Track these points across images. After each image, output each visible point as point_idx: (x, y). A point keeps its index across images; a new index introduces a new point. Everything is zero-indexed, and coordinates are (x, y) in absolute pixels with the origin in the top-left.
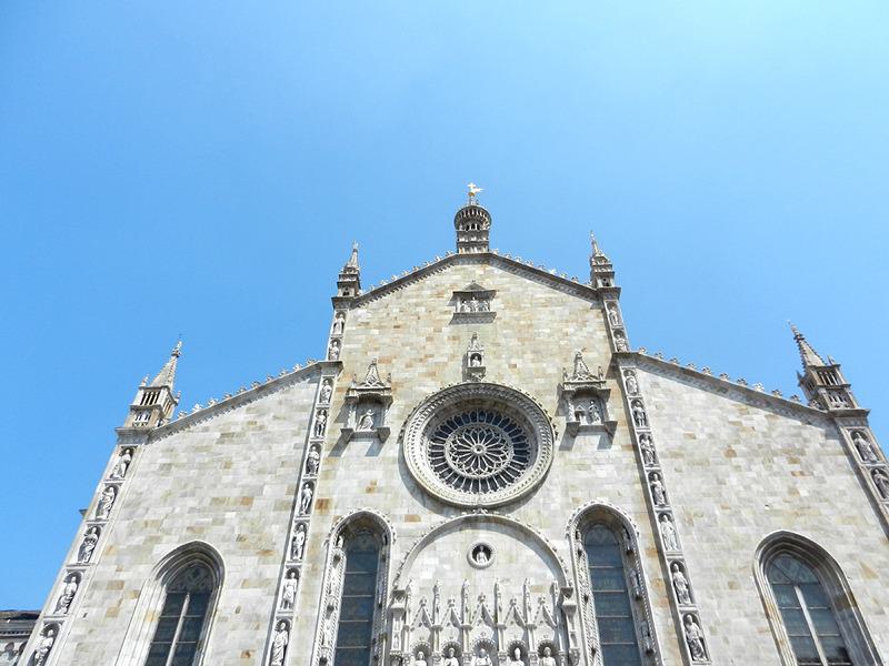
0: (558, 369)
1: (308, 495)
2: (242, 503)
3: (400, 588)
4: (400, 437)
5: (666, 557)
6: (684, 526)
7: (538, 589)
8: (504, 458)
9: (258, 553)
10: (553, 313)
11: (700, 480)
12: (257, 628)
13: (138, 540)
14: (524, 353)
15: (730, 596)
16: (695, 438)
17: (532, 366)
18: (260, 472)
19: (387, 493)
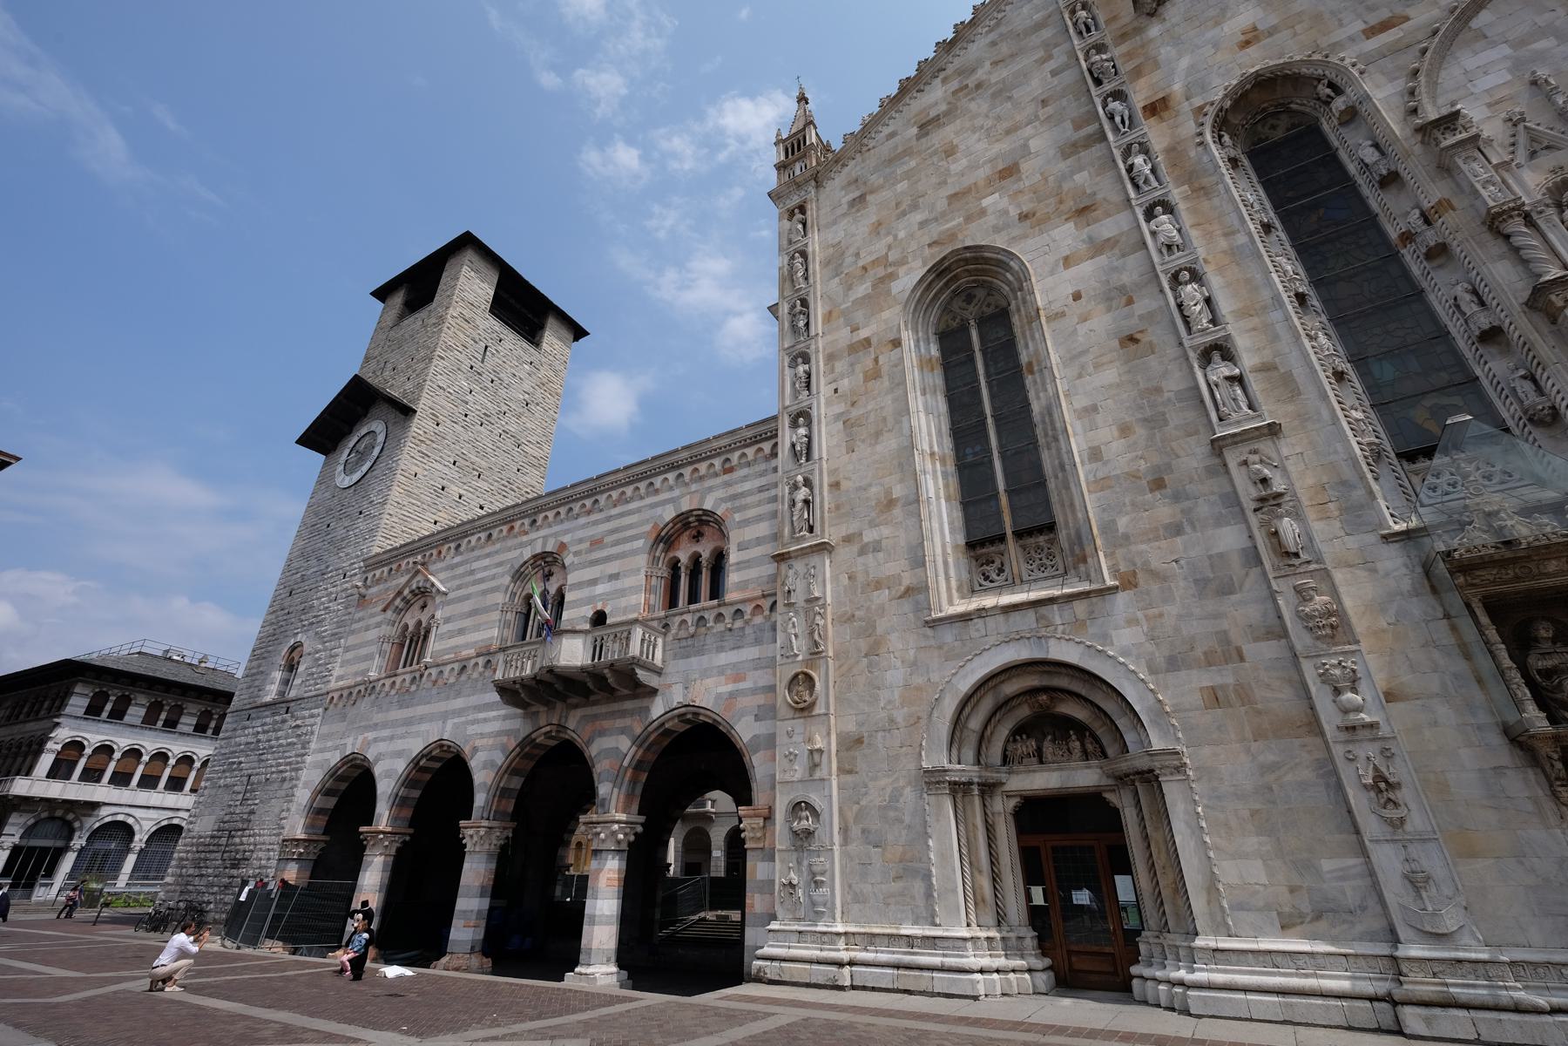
9: (1066, 220)
12: (1130, 302)
13: (863, 289)
19: (1293, 27)
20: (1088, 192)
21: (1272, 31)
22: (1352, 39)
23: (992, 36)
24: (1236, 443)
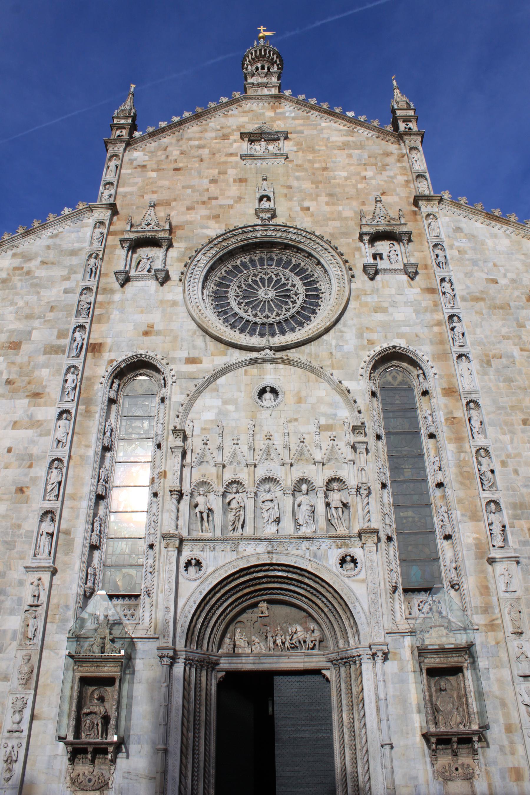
0: (355, 212)
1: (79, 339)
2: (10, 348)
3: (178, 428)
4: (181, 280)
5: (462, 396)
6: (482, 366)
7: (329, 428)
8: (294, 302)
9: (27, 396)
10: (350, 156)
11: (500, 323)
12: (30, 466)
14: (318, 195)
15: (523, 432)
16: (497, 283)
17: (327, 209)
18: (29, 317)
20: (44, 383)
21: (158, 333)
22: (180, 360)
23: (50, 242)
24: (33, 571)
